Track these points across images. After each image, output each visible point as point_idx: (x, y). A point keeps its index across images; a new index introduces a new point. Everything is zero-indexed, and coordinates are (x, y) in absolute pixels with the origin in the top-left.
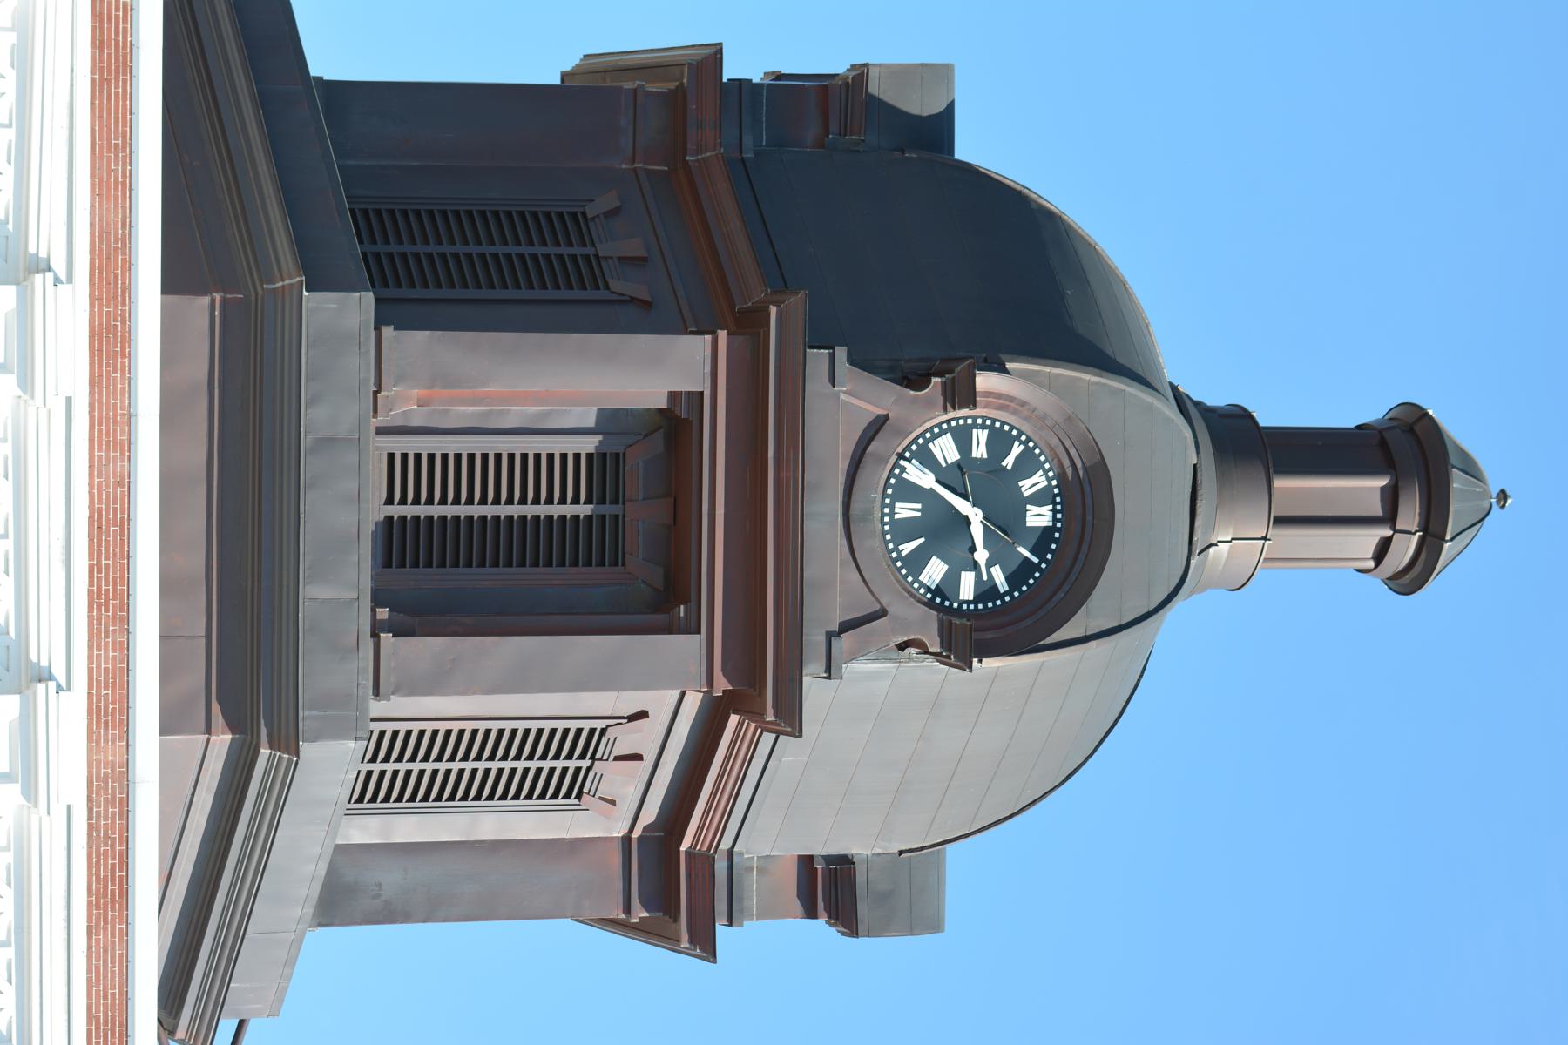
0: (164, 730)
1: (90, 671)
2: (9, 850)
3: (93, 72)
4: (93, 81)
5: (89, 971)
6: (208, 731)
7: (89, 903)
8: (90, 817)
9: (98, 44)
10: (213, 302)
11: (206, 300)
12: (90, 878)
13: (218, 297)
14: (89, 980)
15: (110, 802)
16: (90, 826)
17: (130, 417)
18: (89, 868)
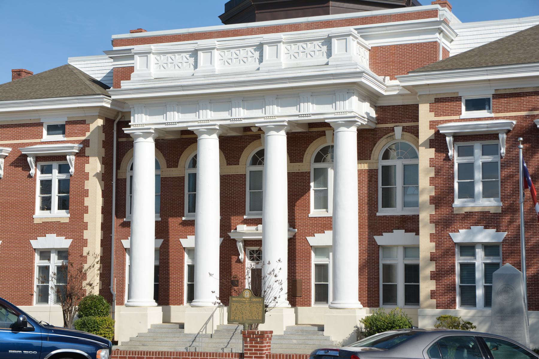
0: (329, 14)
1: (293, 31)
2: (307, 44)
3: (193, 40)
4: (194, 40)
5: (340, 27)
6: (329, 6)
7: (329, 28)
8: (314, 29)
9: (188, 40)
10: (257, 13)
11: (257, 15)
12: (324, 28)
13: (256, 12)
14: (342, 26)
15: (311, 25)
16: (316, 29)
17: (248, 28)
18: (323, 28)
